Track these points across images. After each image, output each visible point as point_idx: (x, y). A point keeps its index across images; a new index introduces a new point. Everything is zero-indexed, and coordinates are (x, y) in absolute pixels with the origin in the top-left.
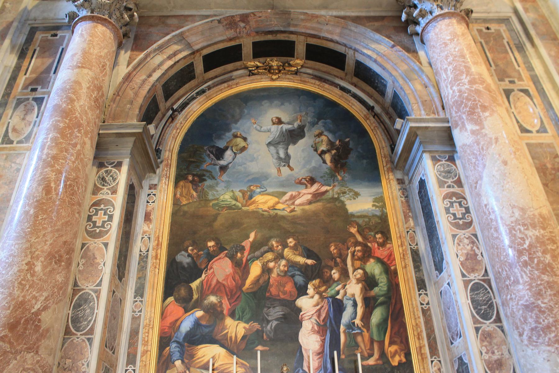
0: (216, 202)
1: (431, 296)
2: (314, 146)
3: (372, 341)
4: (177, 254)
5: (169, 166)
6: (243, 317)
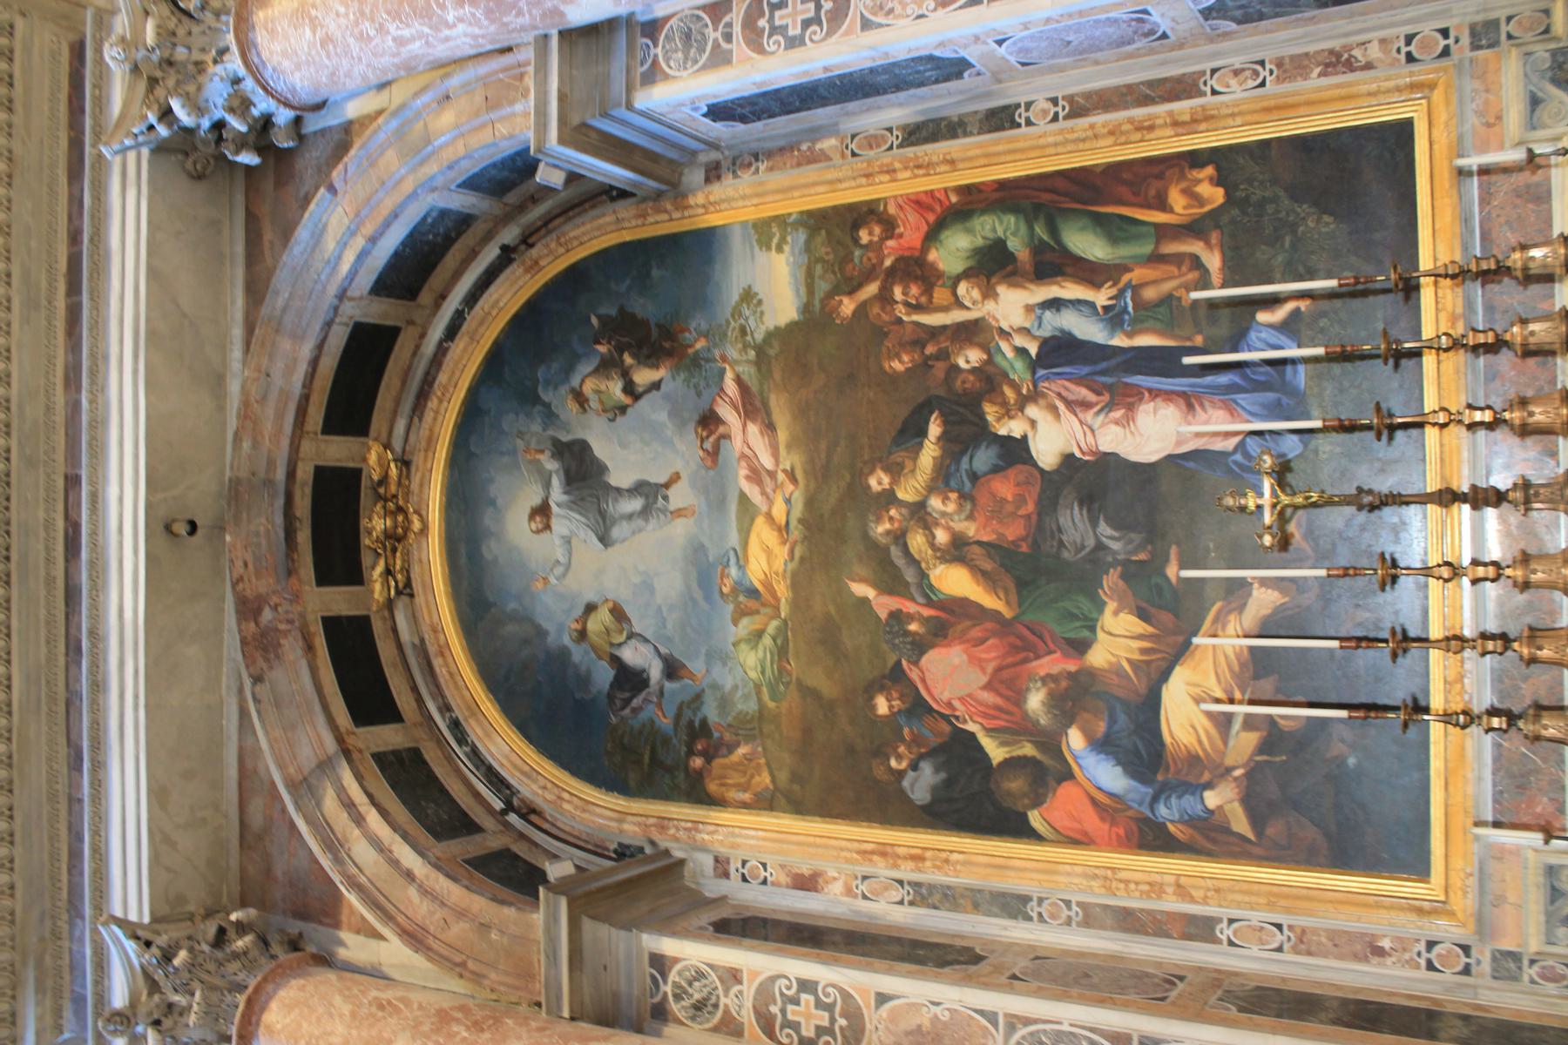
0: (765, 689)
1: (1033, 91)
2: (611, 415)
3: (1156, 259)
4: (910, 801)
5: (663, 823)
6: (1086, 618)
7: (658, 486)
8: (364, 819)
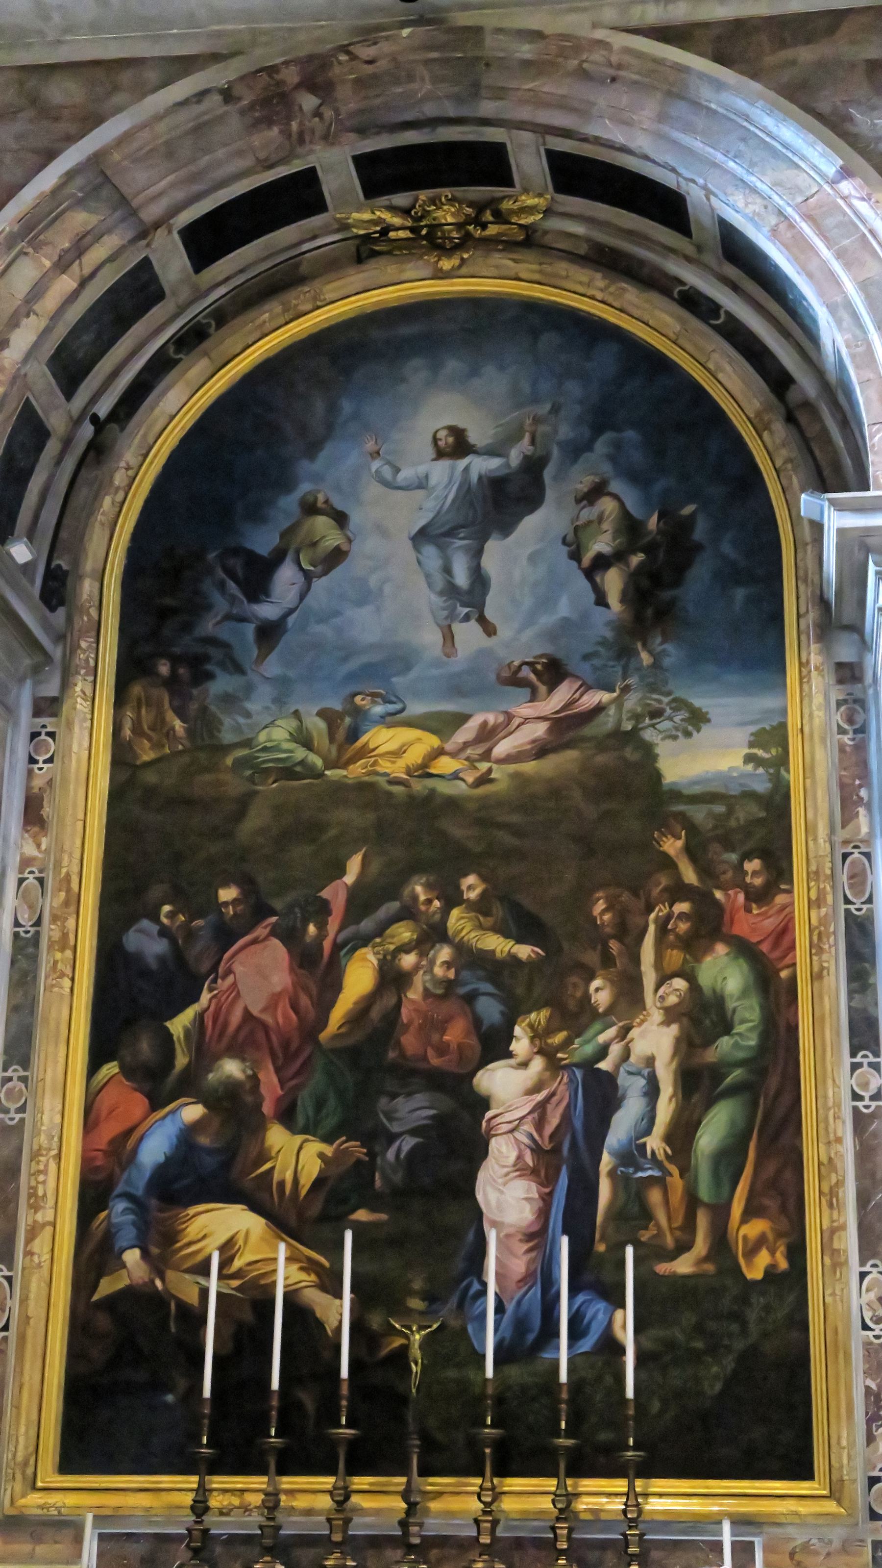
2: (570, 537)
3: (692, 1202)
7: (480, 607)
8: (63, 272)
